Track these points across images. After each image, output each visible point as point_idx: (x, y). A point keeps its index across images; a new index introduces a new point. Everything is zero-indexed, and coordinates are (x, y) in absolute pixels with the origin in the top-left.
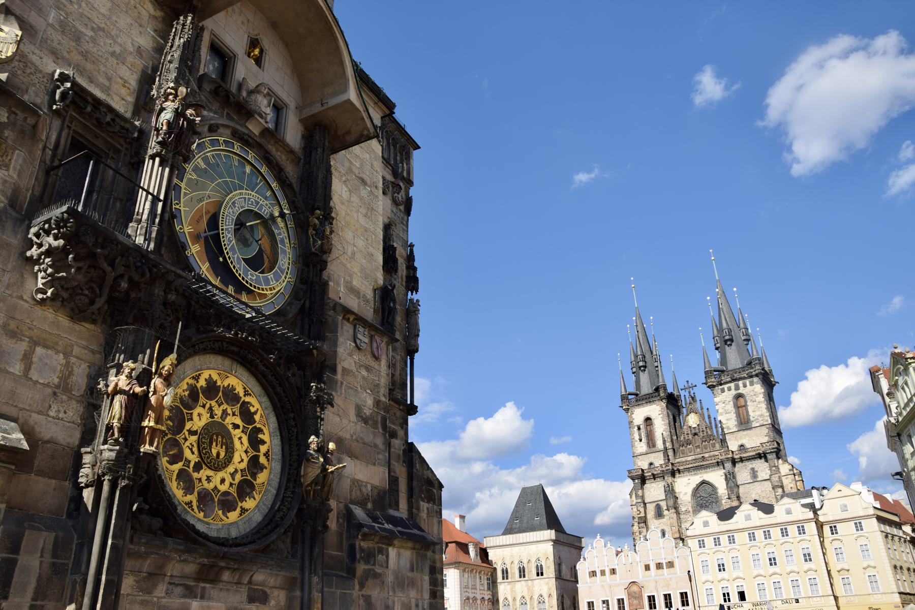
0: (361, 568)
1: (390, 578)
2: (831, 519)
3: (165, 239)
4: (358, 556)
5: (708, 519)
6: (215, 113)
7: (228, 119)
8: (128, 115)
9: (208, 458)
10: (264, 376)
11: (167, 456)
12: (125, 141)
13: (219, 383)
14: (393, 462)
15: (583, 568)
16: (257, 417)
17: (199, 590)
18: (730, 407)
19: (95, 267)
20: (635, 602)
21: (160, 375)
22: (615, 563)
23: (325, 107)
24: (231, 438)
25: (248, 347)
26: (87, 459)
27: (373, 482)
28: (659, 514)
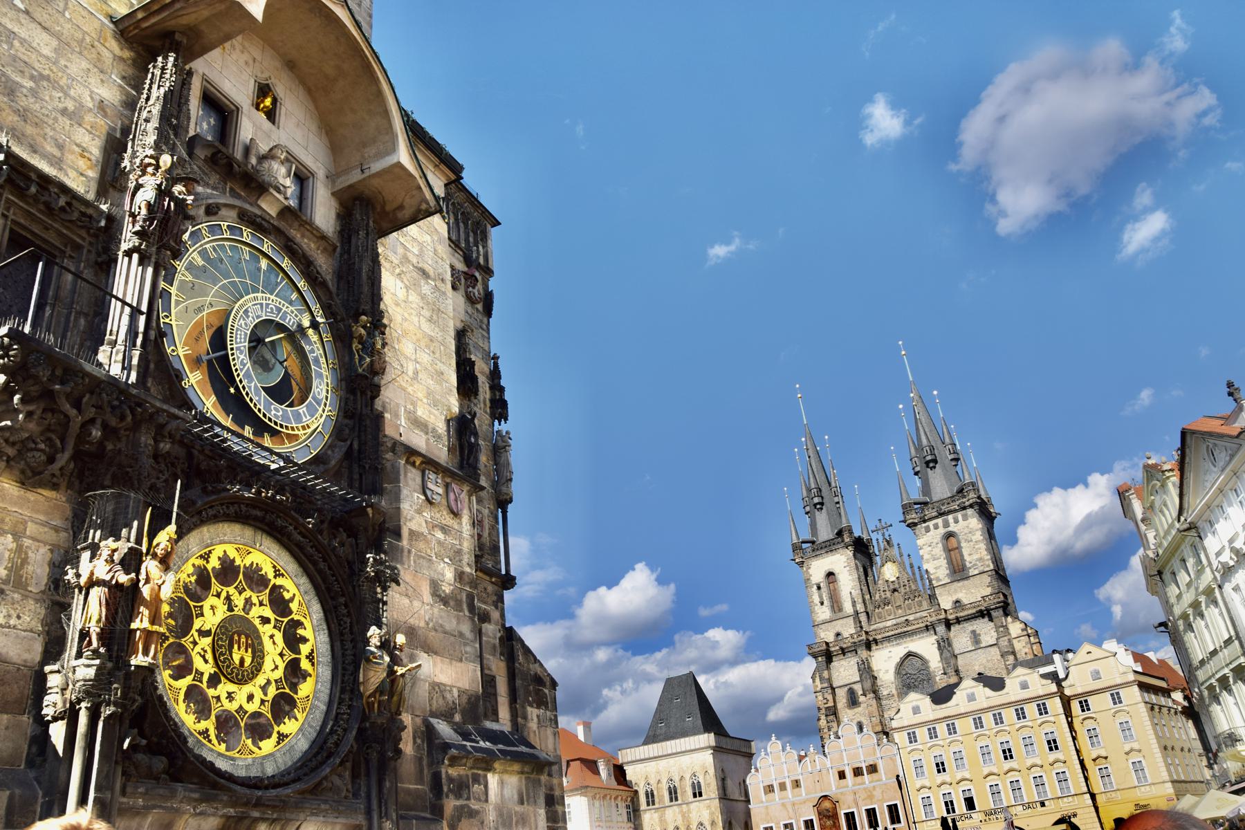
0: (450, 804)
1: (491, 816)
2: (1080, 691)
3: (152, 366)
4: (445, 789)
5: (919, 703)
6: (214, 188)
7: (232, 196)
8: (91, 196)
9: (228, 667)
10: (301, 548)
11: (169, 668)
12: (88, 233)
14: (486, 655)
15: (755, 782)
16: (294, 606)
18: (939, 550)
19: (53, 411)
20: (829, 823)
21: (155, 556)
22: (798, 771)
23: (367, 173)
24: (259, 637)
25: (276, 508)
26: (54, 681)
27: (460, 685)
28: (853, 701)
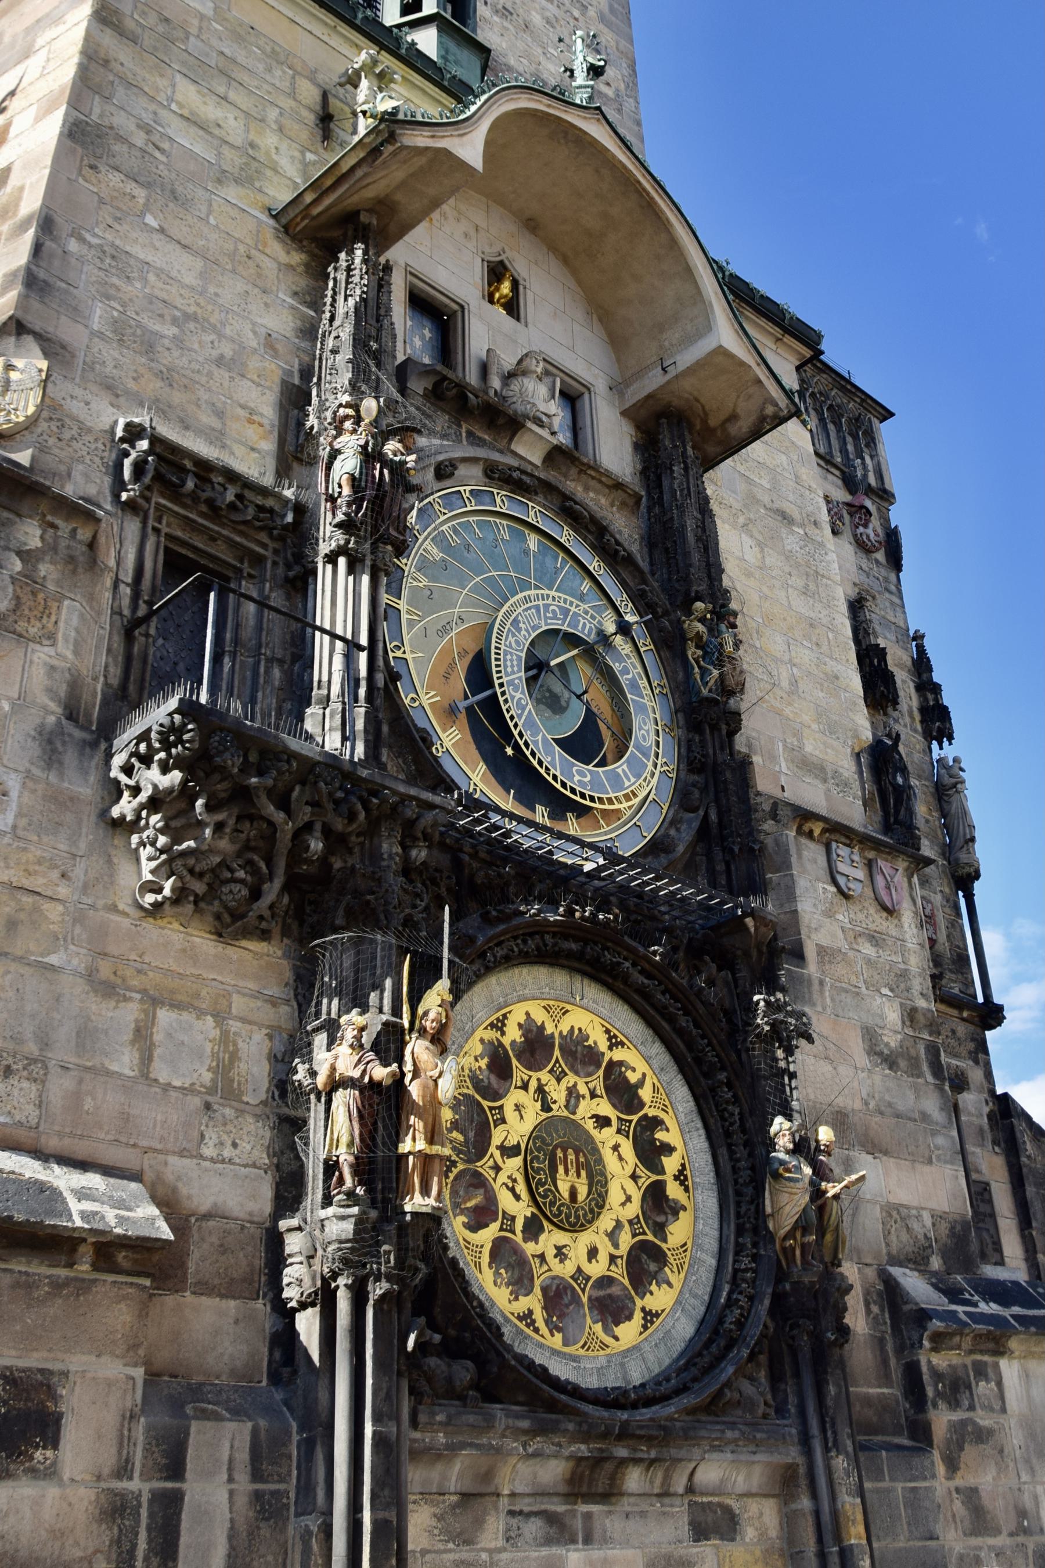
3: (385, 729)
4: (930, 1392)
6: (443, 437)
7: (472, 444)
8: (268, 480)
9: (552, 1204)
12: (271, 536)
13: (550, 1029)
14: (970, 1148)
17: (579, 1524)
19: (251, 818)
21: (422, 1032)
24: (595, 1151)
25: (601, 935)
26: (294, 1244)
27: (933, 1205)
